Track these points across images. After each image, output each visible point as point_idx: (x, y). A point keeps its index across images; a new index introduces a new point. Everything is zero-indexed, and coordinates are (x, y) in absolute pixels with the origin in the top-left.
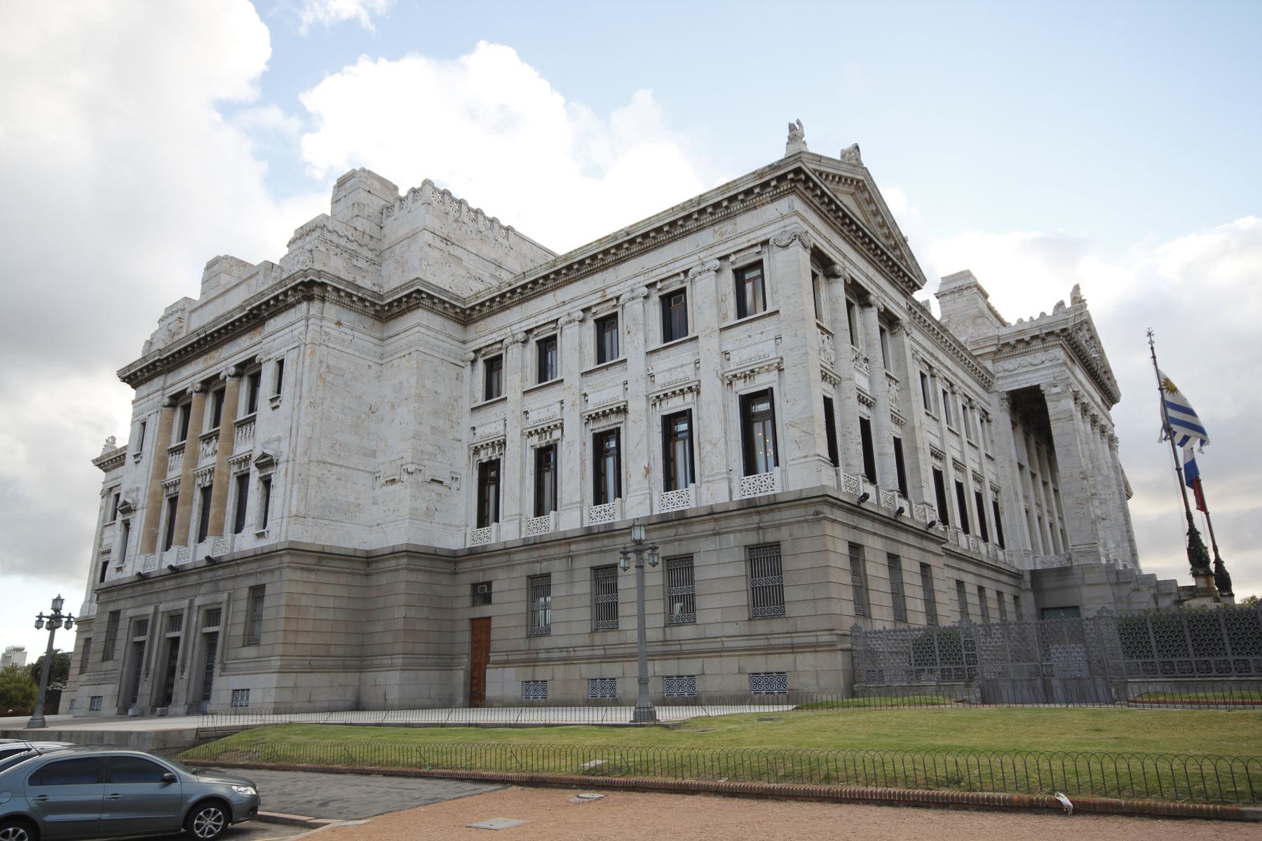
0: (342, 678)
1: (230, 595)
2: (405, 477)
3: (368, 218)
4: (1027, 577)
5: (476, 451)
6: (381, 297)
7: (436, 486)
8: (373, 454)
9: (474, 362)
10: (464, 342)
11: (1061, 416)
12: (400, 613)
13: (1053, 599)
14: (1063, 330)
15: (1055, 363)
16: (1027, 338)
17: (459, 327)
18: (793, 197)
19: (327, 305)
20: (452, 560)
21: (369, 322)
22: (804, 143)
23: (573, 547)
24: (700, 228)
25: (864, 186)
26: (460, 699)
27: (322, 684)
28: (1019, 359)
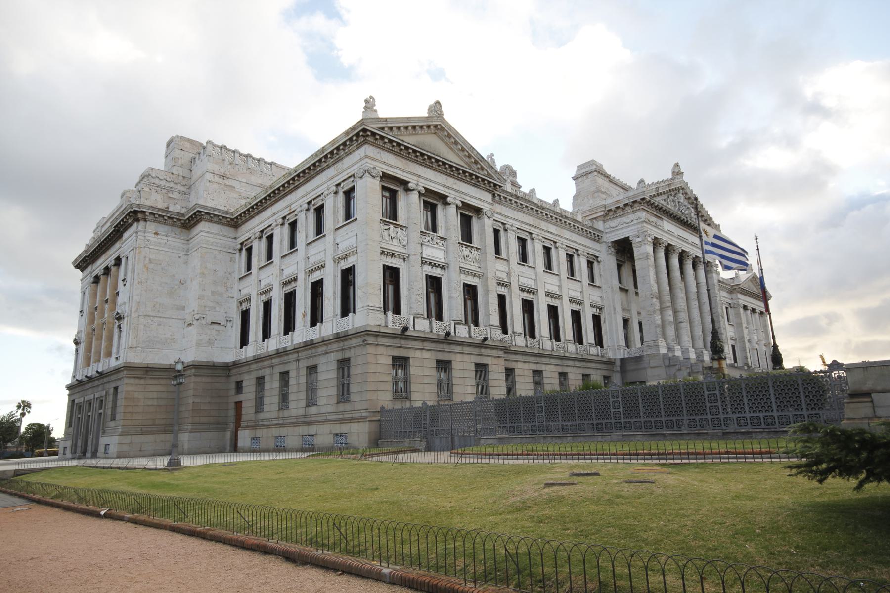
0: (162, 437)
1: (107, 392)
2: (195, 322)
3: (182, 166)
4: (618, 363)
5: (241, 303)
6: (183, 215)
7: (216, 327)
8: (183, 308)
9: (241, 250)
10: (236, 238)
12: (191, 400)
13: (631, 377)
14: (643, 199)
16: (621, 205)
17: (232, 230)
18: (366, 146)
19: (148, 223)
20: (227, 368)
21: (178, 230)
22: (376, 111)
23: (273, 361)
24: (328, 167)
25: (442, 127)
26: (229, 448)
27: (149, 441)
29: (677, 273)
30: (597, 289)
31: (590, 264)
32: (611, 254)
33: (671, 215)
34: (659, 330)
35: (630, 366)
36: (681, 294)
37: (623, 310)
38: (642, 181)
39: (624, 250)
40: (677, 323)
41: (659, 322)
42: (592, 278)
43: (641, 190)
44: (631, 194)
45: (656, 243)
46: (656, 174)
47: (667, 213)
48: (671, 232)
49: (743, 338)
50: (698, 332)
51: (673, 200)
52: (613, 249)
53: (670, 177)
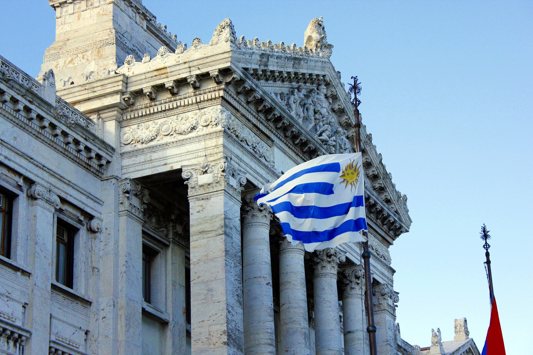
11: (207, 227)
28: (160, 121)
30: (79, 306)
31: (66, 233)
32: (129, 214)
33: (294, 137)
42: (66, 272)
47: (285, 129)
52: (135, 201)
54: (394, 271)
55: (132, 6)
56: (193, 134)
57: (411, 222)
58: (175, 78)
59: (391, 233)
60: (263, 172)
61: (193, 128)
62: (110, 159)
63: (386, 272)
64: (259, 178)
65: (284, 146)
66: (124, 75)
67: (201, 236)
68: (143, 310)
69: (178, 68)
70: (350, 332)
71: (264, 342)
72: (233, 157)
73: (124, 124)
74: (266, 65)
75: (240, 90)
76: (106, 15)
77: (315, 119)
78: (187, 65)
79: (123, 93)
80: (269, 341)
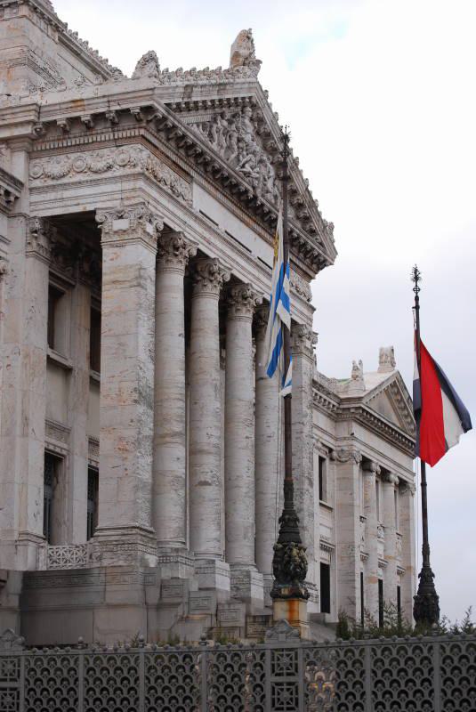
4: (15, 585)
11: (119, 276)
14: (148, 110)
15: (128, 171)
28: (73, 156)
29: (209, 340)
32: (37, 256)
34: (143, 497)
35: (49, 598)
36: (211, 402)
37: (51, 427)
38: (150, 59)
39: (74, 248)
40: (193, 484)
41: (146, 476)
43: (147, 83)
44: (113, 88)
45: (166, 242)
46: (196, 49)
48: (207, 219)
49: (351, 546)
50: (244, 514)
51: (226, 133)
52: (43, 241)
53: (225, 63)
54: (314, 309)
55: (44, 18)
56: (109, 174)
57: (337, 253)
58: (92, 112)
59: (314, 266)
60: (180, 213)
61: (110, 168)
62: (17, 194)
63: (305, 311)
64: (176, 220)
65: (203, 182)
66: (36, 104)
67: (114, 285)
68: (48, 356)
69: (96, 101)
70: (262, 379)
71: (174, 396)
72: (151, 201)
73: (33, 155)
74: (190, 97)
75: (161, 127)
76: (17, 29)
77: (238, 148)
78: (106, 99)
79: (34, 123)
80: (179, 397)
